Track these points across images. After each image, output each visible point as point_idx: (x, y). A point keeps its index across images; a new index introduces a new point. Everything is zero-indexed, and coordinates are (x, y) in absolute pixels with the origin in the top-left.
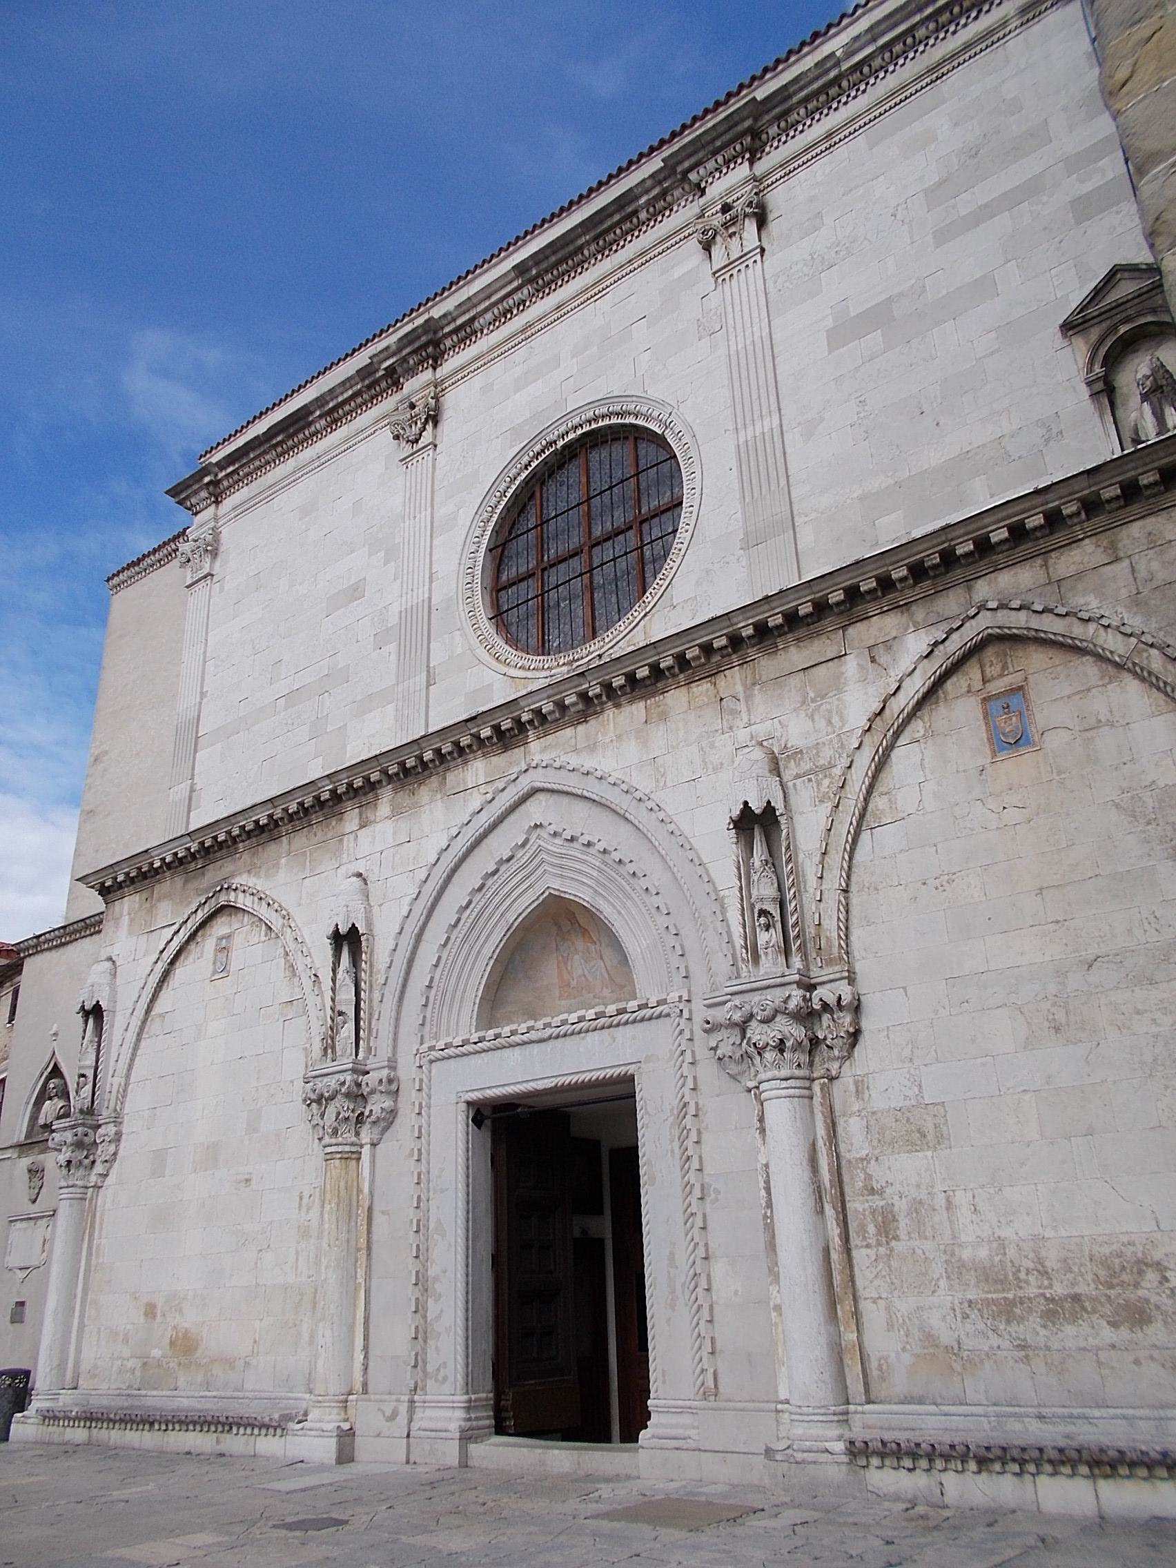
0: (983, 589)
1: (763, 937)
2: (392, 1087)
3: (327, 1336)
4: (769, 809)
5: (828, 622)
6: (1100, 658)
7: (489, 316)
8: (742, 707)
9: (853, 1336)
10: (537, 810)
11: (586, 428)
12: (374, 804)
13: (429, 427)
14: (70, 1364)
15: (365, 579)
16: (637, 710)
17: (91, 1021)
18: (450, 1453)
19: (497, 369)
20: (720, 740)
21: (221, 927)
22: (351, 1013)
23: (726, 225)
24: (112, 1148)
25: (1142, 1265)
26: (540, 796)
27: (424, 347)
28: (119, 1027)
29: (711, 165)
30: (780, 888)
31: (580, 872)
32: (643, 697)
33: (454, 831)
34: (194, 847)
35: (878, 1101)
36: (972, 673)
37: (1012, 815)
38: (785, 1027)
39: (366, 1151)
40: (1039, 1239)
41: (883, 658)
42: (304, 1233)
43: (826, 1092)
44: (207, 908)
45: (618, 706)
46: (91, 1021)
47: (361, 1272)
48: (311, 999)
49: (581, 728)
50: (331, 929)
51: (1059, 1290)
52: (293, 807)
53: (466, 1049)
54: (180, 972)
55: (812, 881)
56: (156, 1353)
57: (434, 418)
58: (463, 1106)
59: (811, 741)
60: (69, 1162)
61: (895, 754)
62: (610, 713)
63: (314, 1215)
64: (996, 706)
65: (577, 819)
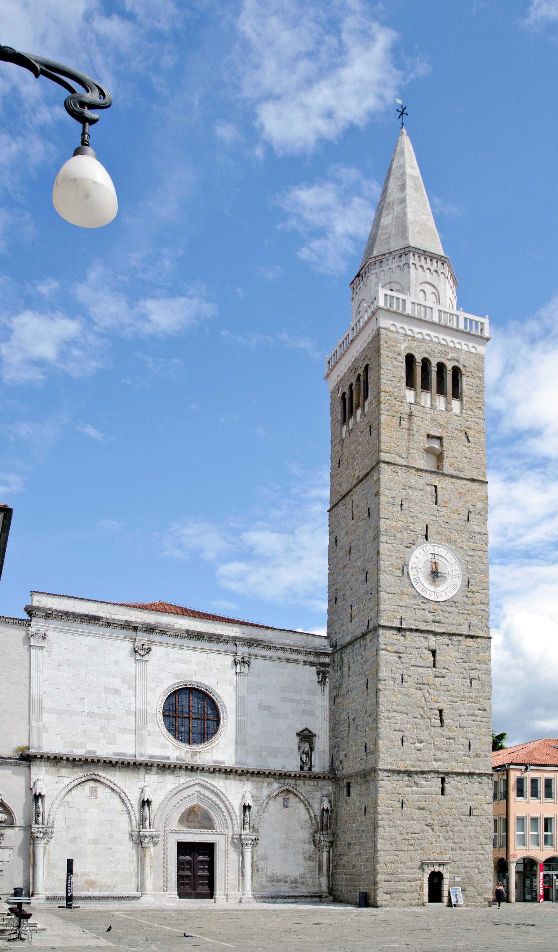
0: (287, 781)
5: (263, 776)
6: (300, 798)
10: (198, 788)
16: (224, 775)
20: (240, 789)
25: (288, 876)
26: (199, 785)
31: (205, 803)
32: (226, 774)
35: (259, 853)
36: (283, 794)
37: (284, 817)
38: (250, 842)
40: (277, 873)
41: (270, 785)
45: (219, 773)
49: (210, 774)
51: (278, 879)
53: (176, 832)
59: (257, 795)
61: (270, 802)
64: (285, 800)
65: (207, 793)
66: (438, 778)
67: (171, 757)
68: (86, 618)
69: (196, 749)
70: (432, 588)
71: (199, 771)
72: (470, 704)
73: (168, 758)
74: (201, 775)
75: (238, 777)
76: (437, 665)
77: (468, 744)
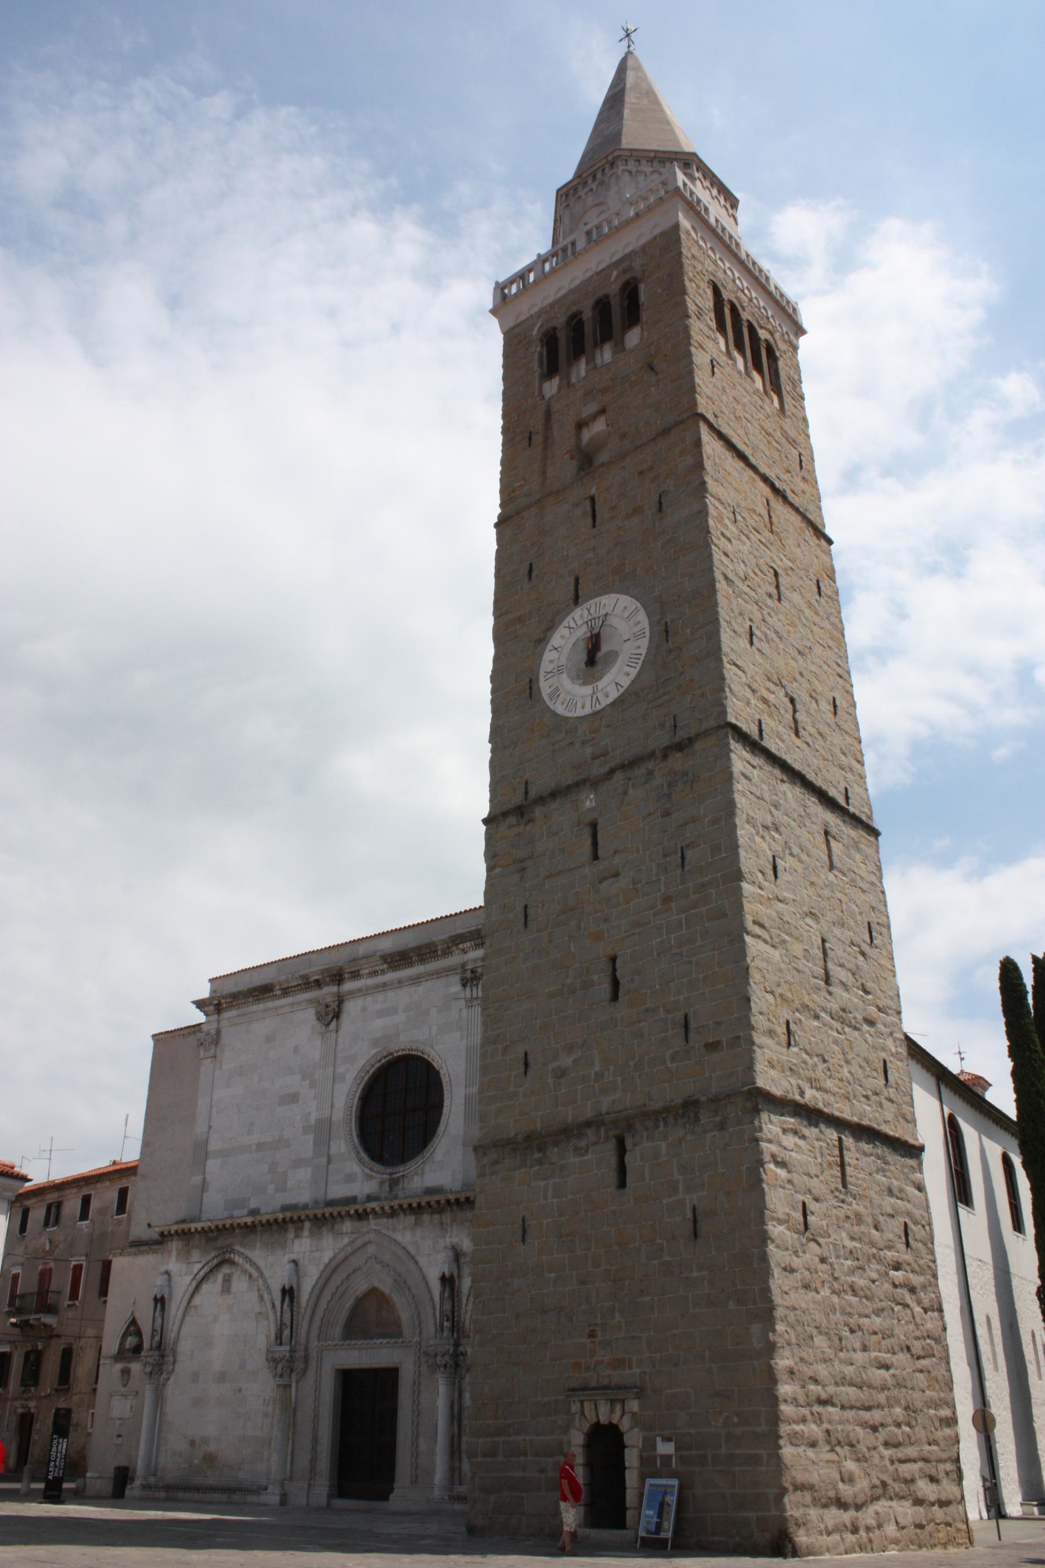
1: (446, 1324)
2: (306, 1359)
3: (275, 1457)
4: (452, 1276)
7: (367, 971)
8: (449, 1229)
9: (457, 1464)
11: (407, 1052)
12: (302, 1228)
13: (335, 1020)
14: (153, 1464)
15: (299, 1093)
16: (411, 1219)
17: (159, 1305)
18: (323, 1501)
19: (369, 999)
20: (441, 1241)
21: (226, 1270)
22: (289, 1324)
23: (472, 979)
24: (171, 1367)
27: (335, 975)
28: (175, 1309)
29: (468, 944)
30: (453, 1307)
33: (336, 1251)
34: (213, 1227)
39: (294, 1384)
42: (266, 1415)
43: (460, 1382)
44: (219, 1259)
45: (405, 1214)
46: (159, 1305)
47: (290, 1433)
48: (271, 1314)
49: (390, 1221)
50: (281, 1287)
52: (264, 1221)
54: (206, 1287)
55: (464, 1307)
56: (196, 1461)
57: (337, 1016)
58: (334, 1371)
60: (151, 1373)
62: (402, 1214)
63: (270, 1408)
66: (607, 1139)
67: (359, 1197)
68: (257, 993)
69: (399, 1172)
70: (588, 690)
71: (371, 1216)
72: (683, 916)
73: (353, 1200)
74: (376, 1224)
75: (437, 1216)
76: (600, 853)
77: (683, 1021)
